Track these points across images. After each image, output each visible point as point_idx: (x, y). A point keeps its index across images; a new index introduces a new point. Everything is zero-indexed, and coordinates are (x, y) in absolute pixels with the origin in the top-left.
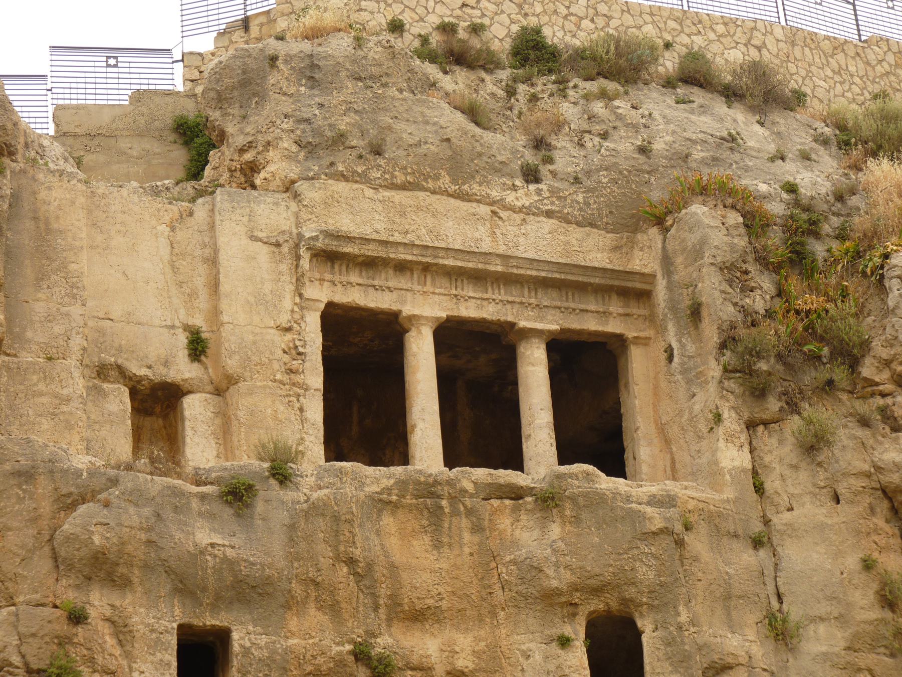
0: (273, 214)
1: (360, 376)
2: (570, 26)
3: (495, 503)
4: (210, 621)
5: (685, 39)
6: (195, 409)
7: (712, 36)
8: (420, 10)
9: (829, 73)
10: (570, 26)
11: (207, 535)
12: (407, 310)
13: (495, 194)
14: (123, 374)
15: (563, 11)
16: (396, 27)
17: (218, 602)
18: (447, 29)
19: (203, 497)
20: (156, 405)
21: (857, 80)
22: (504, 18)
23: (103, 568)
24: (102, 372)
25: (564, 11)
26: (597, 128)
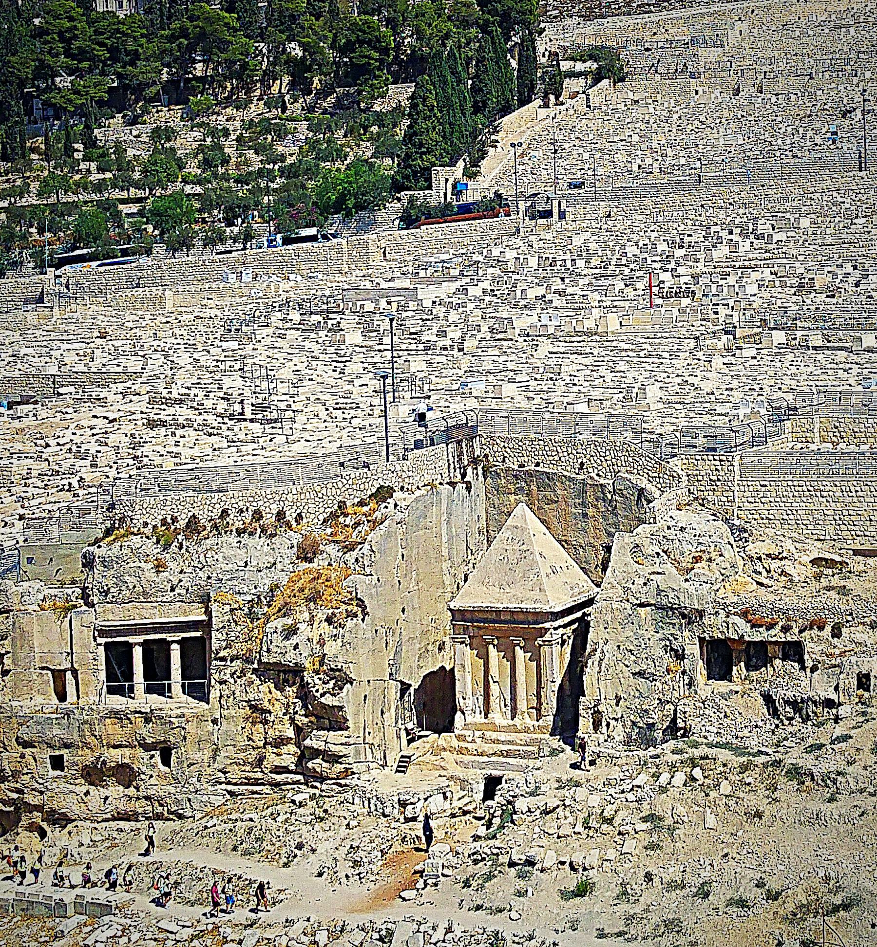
0: (89, 617)
1: (118, 660)
2: (210, 508)
3: (137, 715)
4: (57, 753)
5: (255, 504)
6: (69, 674)
7: (266, 500)
8: (156, 515)
9: (317, 499)
10: (210, 508)
11: (56, 732)
12: (131, 641)
13: (159, 600)
14: (48, 669)
15: (208, 503)
16: (146, 524)
17: (59, 749)
18: (164, 522)
19: (56, 719)
20: (59, 676)
21: (331, 497)
22: (186, 511)
23: (26, 745)
24: (43, 668)
25: (208, 503)
26: (200, 566)
